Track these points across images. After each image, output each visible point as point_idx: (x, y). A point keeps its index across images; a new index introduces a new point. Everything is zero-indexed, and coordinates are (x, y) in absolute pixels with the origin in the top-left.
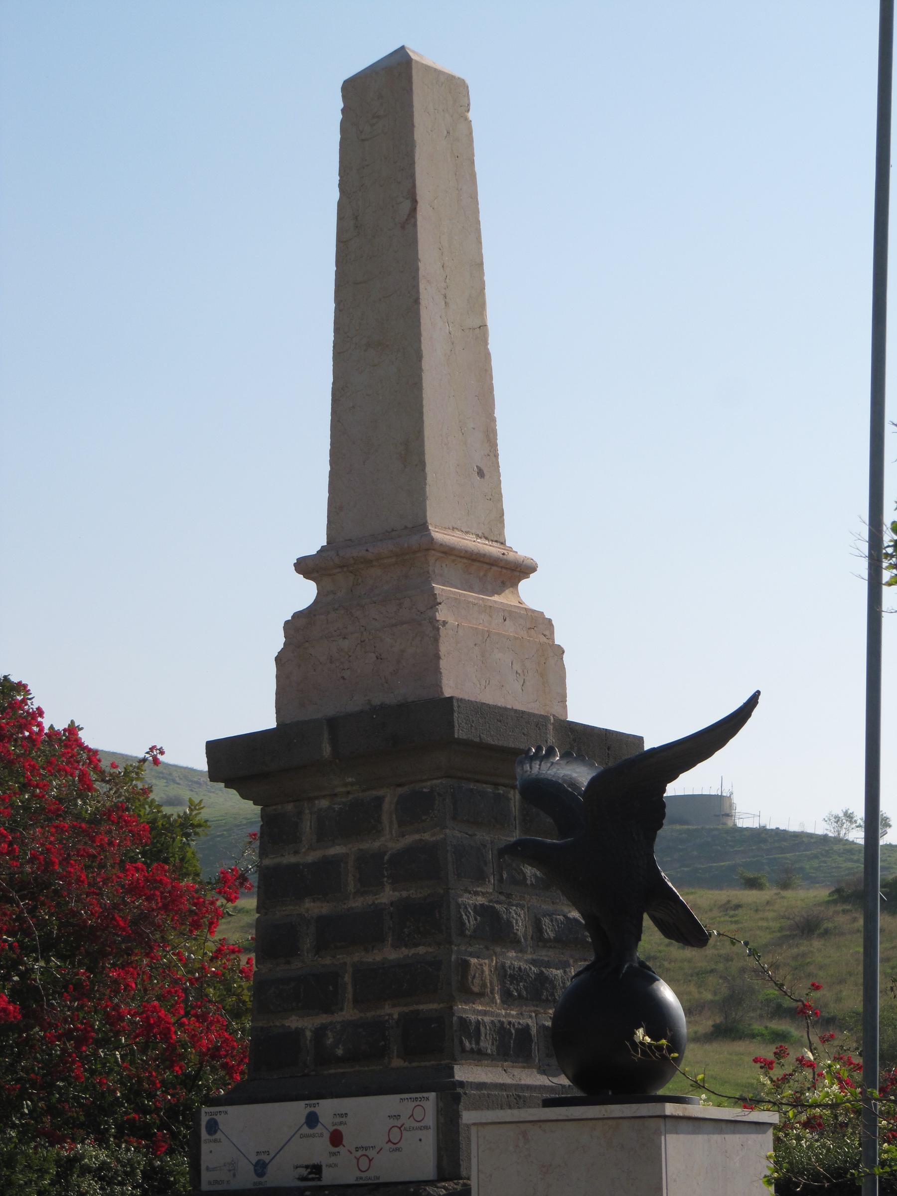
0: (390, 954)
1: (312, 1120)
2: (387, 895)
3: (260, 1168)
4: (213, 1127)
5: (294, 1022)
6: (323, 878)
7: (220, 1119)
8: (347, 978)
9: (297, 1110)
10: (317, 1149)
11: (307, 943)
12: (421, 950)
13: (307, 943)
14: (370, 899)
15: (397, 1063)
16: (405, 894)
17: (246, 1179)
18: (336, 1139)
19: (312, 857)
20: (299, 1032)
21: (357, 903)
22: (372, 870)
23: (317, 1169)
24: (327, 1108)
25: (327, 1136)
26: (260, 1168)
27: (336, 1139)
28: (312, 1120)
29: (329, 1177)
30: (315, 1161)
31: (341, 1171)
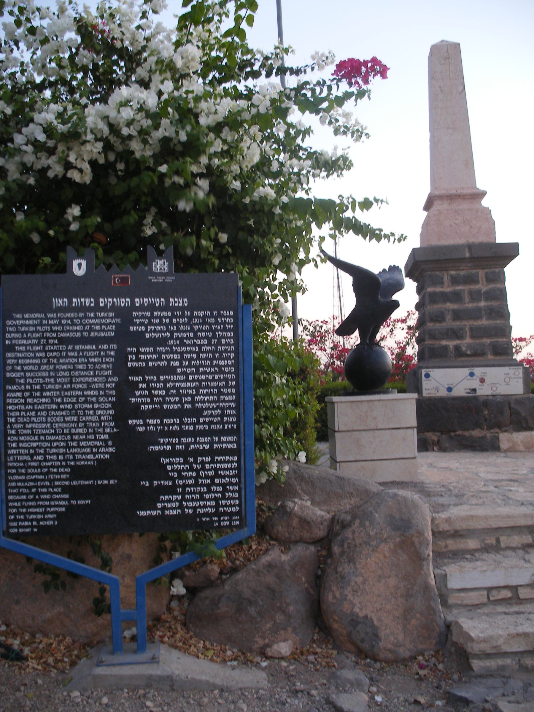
0: (484, 322)
1: (472, 374)
2: (482, 304)
3: (450, 389)
4: (427, 376)
5: (444, 343)
6: (456, 297)
7: (431, 373)
8: (467, 329)
9: (467, 371)
10: (475, 383)
11: (449, 317)
12: (498, 322)
13: (449, 317)
14: (475, 304)
15: (490, 357)
16: (490, 303)
17: (443, 393)
18: (482, 381)
19: (449, 290)
20: (446, 347)
21: (470, 305)
22: (475, 296)
23: (474, 390)
24: (478, 371)
25: (478, 380)
26: (450, 389)
27: (482, 381)
28: (472, 374)
29: (479, 393)
30: (473, 387)
31: (484, 391)
